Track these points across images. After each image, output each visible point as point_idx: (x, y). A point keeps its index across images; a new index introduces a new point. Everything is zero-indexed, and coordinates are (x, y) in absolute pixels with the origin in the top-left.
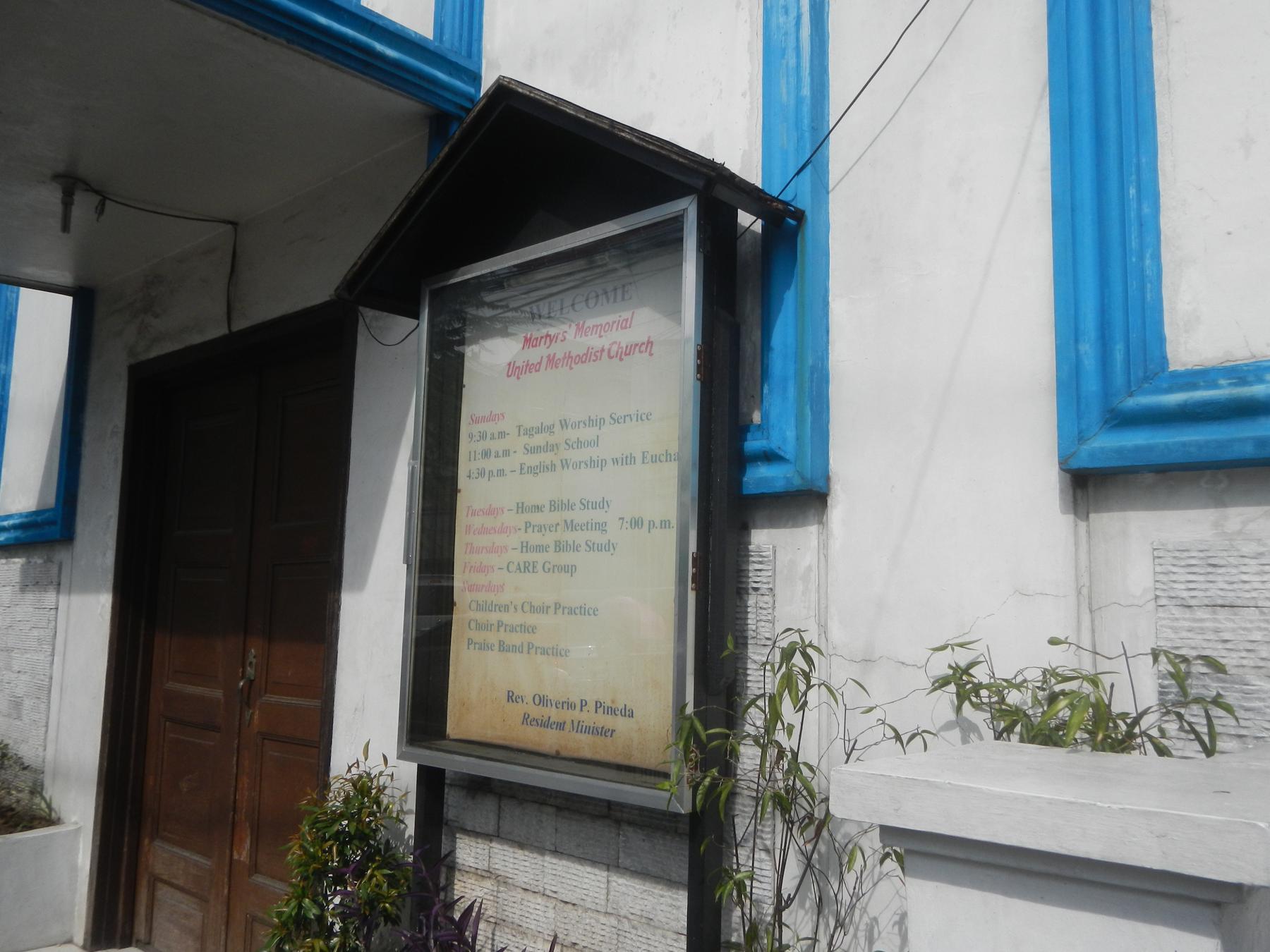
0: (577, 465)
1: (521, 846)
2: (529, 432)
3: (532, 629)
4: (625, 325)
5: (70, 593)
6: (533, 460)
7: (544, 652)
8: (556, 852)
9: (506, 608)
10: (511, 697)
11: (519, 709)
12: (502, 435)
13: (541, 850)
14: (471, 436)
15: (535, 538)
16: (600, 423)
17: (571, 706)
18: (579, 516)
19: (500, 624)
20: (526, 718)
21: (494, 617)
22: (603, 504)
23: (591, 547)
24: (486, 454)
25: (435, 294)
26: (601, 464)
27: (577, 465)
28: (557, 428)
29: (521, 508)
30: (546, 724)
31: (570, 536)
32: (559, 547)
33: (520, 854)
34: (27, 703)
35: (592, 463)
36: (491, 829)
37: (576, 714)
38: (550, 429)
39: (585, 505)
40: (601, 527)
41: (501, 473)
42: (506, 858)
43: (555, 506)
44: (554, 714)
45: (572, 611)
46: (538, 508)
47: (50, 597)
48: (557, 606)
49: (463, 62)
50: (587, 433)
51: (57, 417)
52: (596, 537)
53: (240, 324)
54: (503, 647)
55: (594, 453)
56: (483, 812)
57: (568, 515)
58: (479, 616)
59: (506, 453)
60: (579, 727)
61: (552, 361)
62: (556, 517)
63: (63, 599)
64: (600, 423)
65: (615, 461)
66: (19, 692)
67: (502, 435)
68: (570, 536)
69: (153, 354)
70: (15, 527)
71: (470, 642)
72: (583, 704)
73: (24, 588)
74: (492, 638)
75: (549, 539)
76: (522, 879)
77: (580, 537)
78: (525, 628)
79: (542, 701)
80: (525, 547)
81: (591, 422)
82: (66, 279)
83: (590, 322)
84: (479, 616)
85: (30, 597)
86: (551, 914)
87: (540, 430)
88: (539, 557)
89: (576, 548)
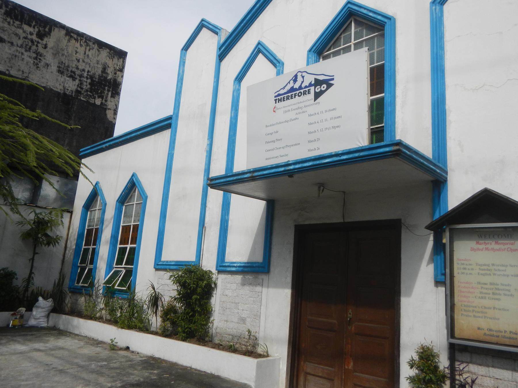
0: (499, 275)
1: (480, 365)
2: (481, 265)
3: (486, 313)
4: (512, 244)
5: (268, 287)
6: (483, 272)
7: (490, 318)
8: (493, 367)
9: (475, 307)
10: (479, 329)
11: (483, 332)
12: (470, 265)
13: (488, 366)
14: (458, 264)
15: (485, 291)
16: (506, 266)
17: (501, 332)
18: (501, 287)
19: (473, 311)
20: (485, 334)
21: (471, 309)
22: (509, 285)
23: (505, 295)
24: (465, 269)
25: (451, 230)
26: (508, 276)
27: (499, 275)
28: (491, 265)
29: (479, 283)
30: (493, 336)
31: (497, 292)
32: (493, 294)
33: (480, 367)
34: (248, 320)
35: (504, 275)
36: (469, 360)
37: (503, 334)
38: (488, 265)
39: (502, 285)
40: (509, 291)
41: (471, 274)
42: (473, 368)
43: (491, 284)
44: (495, 334)
45: (500, 309)
46: (485, 284)
47: (258, 289)
48: (494, 308)
49: (443, 167)
50: (503, 268)
51: (257, 235)
52: (507, 293)
53: (347, 220)
54: (475, 316)
55: (505, 273)
56: (466, 356)
57: (497, 287)
58: (465, 308)
59: (472, 269)
60: (504, 337)
61: (487, 249)
62: (492, 287)
63: (265, 290)
64: (506, 266)
65: (512, 276)
66: (243, 316)
67: (470, 265)
68: (497, 292)
69: (307, 223)
70: (239, 267)
71: (462, 314)
72: (505, 332)
73: (243, 284)
74: (471, 314)
75: (490, 292)
76: (480, 373)
77: (502, 292)
78: (482, 312)
79: (490, 330)
80: (481, 293)
81: (503, 266)
82: (262, 195)
83: (500, 242)
84: (465, 308)
85: (247, 288)
86: (492, 382)
87: (485, 265)
88: (487, 296)
89: (500, 295)
